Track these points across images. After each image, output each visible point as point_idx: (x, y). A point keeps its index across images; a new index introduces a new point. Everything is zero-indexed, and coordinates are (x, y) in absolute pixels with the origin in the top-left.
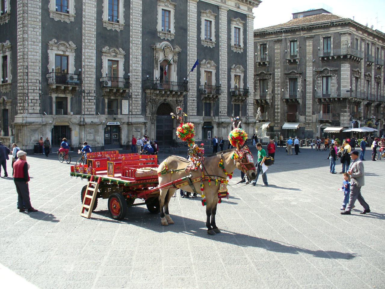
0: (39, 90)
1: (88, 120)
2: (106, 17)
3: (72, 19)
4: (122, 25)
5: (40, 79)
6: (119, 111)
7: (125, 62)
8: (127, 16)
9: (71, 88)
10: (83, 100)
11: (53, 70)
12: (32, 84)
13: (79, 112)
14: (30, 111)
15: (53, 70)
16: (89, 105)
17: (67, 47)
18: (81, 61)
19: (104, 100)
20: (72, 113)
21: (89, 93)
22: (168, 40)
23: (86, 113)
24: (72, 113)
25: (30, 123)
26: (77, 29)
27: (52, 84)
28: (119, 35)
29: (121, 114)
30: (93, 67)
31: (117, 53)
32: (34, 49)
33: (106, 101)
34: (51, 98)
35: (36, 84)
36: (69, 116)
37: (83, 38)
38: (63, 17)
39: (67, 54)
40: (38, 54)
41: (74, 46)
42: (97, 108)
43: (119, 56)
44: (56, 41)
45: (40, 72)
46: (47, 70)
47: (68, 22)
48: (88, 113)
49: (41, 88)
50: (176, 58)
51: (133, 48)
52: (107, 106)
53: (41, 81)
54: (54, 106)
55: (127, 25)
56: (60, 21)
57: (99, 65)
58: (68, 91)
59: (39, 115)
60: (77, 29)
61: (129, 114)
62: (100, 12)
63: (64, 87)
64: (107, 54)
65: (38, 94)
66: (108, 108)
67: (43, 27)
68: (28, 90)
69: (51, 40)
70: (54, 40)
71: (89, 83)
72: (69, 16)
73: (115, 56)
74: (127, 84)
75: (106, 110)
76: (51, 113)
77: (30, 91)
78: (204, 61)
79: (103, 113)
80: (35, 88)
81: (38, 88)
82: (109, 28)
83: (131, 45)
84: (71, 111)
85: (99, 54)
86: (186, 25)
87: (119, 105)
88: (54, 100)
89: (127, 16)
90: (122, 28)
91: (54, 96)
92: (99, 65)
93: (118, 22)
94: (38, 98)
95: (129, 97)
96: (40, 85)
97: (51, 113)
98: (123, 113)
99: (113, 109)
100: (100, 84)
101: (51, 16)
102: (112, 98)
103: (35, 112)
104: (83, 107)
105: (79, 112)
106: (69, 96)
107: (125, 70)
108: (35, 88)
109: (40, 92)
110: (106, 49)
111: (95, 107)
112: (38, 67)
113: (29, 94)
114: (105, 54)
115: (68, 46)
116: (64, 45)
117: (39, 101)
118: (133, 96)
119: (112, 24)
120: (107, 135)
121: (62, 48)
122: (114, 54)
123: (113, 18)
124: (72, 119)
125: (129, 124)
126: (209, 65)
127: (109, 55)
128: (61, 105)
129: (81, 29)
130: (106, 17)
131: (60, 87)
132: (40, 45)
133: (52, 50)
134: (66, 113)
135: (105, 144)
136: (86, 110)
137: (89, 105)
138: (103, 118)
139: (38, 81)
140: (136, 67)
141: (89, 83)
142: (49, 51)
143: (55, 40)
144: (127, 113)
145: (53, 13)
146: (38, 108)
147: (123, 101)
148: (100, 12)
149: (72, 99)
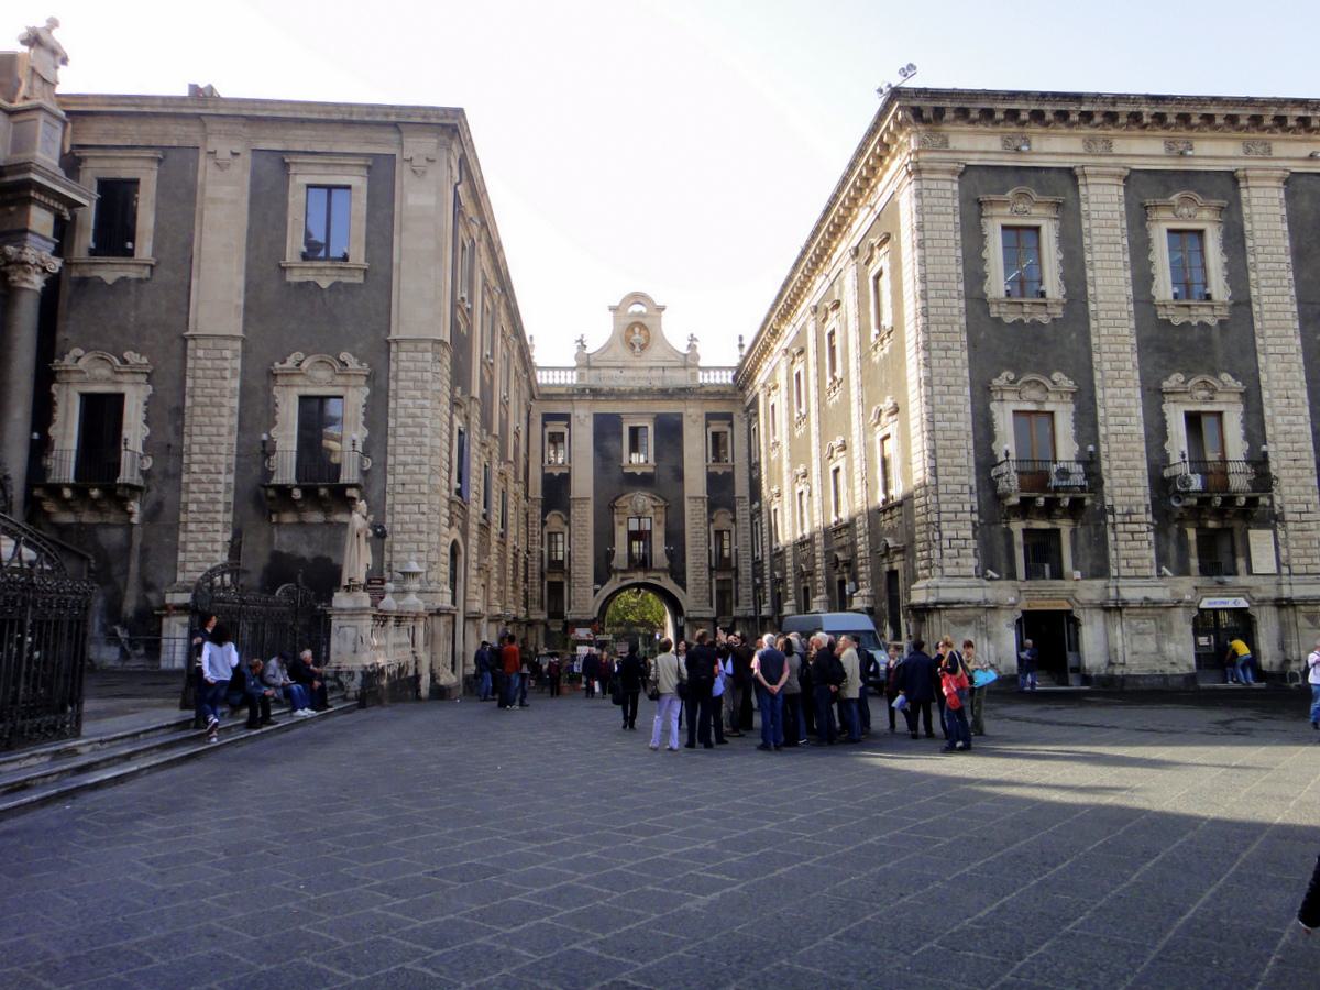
0: (972, 512)
1: (1132, 594)
2: (1164, 288)
3: (1058, 312)
4: (1224, 304)
5: (973, 482)
6: (1241, 563)
7: (1247, 414)
8: (1238, 273)
9: (1066, 502)
10: (1111, 537)
11: (1007, 454)
12: (949, 497)
13: (1100, 570)
14: (948, 571)
15: (1007, 454)
16: (1133, 546)
17: (1047, 390)
18: (1095, 425)
19: (1182, 534)
20: (1078, 574)
21: (1129, 513)
23: (1124, 572)
24: (1078, 574)
25: (949, 605)
26: (1074, 336)
27: (1007, 495)
28: (1216, 335)
29: (1250, 572)
30: (1135, 438)
31: (1214, 390)
32: (950, 403)
33: (1192, 534)
34: (1009, 534)
35: (962, 497)
36: (1067, 585)
37: (1096, 358)
38: (1027, 310)
39: (1048, 407)
40: (962, 416)
41: (1068, 384)
42: (1162, 559)
43: (1224, 397)
44: (1012, 377)
45: (972, 464)
46: (992, 455)
47: (1045, 319)
48: (1132, 572)
49: (976, 508)
51: (1273, 367)
52: (1194, 549)
53: (975, 488)
54: (1020, 554)
55: (1242, 303)
56: (1021, 321)
57: (1157, 432)
58: (1058, 512)
59: (974, 581)
60: (1074, 336)
61: (1279, 573)
62: (1143, 279)
63: (1046, 499)
64: (1178, 397)
65: (970, 526)
66: (1200, 556)
67: (973, 345)
68: (939, 513)
69: (997, 375)
70: (1004, 374)
71: (1127, 483)
72: (1045, 304)
74: (1263, 478)
75: (1194, 562)
76: (1012, 576)
77: (943, 516)
79: (1183, 570)
80: (959, 507)
81: (967, 507)
82: (1177, 321)
83: (1262, 359)
84: (1076, 567)
85: (1154, 396)
87: (1239, 545)
88: (1018, 538)
89: (1238, 273)
90: (1224, 313)
91: (1017, 527)
92: (1157, 432)
93: (1208, 297)
94: (969, 534)
96: (975, 499)
97: (1012, 576)
98: (1256, 569)
99: (1219, 556)
100: (1162, 487)
101: (994, 311)
102: (1211, 524)
103: (963, 571)
104: (1113, 554)
105: (1100, 570)
106: (1065, 527)
107: (1248, 437)
108: (959, 507)
109: (976, 517)
110: (1174, 381)
111: (1152, 554)
112: (964, 452)
113: (944, 525)
114: (1172, 398)
115: (1049, 385)
116: (1039, 383)
117: (972, 544)
118: (1289, 517)
119: (1188, 306)
120: (1203, 641)
121: (1035, 394)
122: (1205, 393)
124: (1075, 589)
125: (1282, 604)
127: (1186, 397)
128: (1043, 553)
129: (1086, 335)
130: (1164, 288)
131: (1033, 500)
132: (967, 391)
133: (1002, 400)
134: (1058, 574)
135: (1199, 666)
136: (1124, 563)
137: (1133, 546)
138: (1186, 587)
139: (966, 489)
140: (1291, 424)
141: (1127, 483)
142: (994, 406)
143: (1008, 375)
144: (1273, 569)
145: (998, 302)
146: (973, 562)
147: (1251, 532)
148: (1143, 279)
149: (1074, 532)
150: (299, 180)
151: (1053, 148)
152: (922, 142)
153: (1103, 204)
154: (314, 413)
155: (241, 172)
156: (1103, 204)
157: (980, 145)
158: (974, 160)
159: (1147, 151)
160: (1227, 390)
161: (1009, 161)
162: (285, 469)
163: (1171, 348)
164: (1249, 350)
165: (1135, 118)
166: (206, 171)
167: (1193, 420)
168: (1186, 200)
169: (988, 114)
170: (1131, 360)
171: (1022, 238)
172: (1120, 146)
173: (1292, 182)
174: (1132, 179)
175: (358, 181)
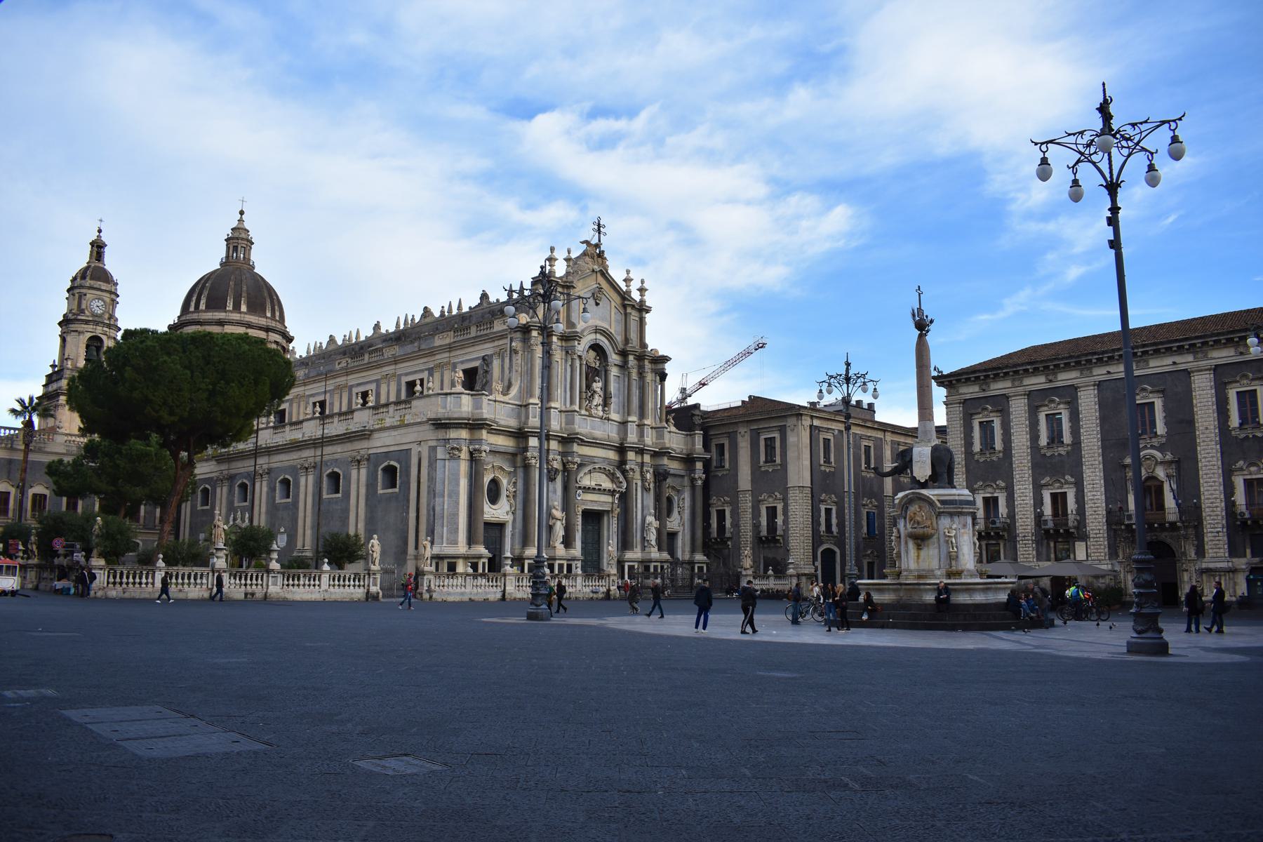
8: (1076, 431)
22: (1153, 447)
41: (1003, 484)
47: (994, 459)
50: (1172, 471)
55: (1077, 443)
57: (1038, 502)
62: (1034, 437)
71: (1025, 524)
73: (1061, 488)
74: (1082, 522)
75: (1052, 556)
78: (1241, 463)
85: (1038, 488)
86: (1192, 414)
89: (1076, 431)
92: (1038, 502)
95: (1084, 537)
107: (1077, 502)
121: (990, 490)
123: (1055, 438)
126: (1253, 469)
141: (1025, 524)
148: (1034, 437)
150: (763, 437)
151: (998, 387)
152: (948, 392)
153: (1018, 408)
154: (772, 512)
155: (747, 437)
156: (1018, 408)
157: (971, 391)
158: (968, 397)
159: (1037, 382)
160: (1067, 482)
161: (981, 395)
162: (764, 533)
163: (1043, 466)
164: (1079, 464)
165: (1026, 371)
166: (740, 439)
167: (1054, 497)
168: (1053, 401)
169: (968, 380)
170: (1027, 474)
171: (986, 427)
172: (1027, 381)
173: (1099, 385)
174: (1029, 395)
175: (776, 435)
